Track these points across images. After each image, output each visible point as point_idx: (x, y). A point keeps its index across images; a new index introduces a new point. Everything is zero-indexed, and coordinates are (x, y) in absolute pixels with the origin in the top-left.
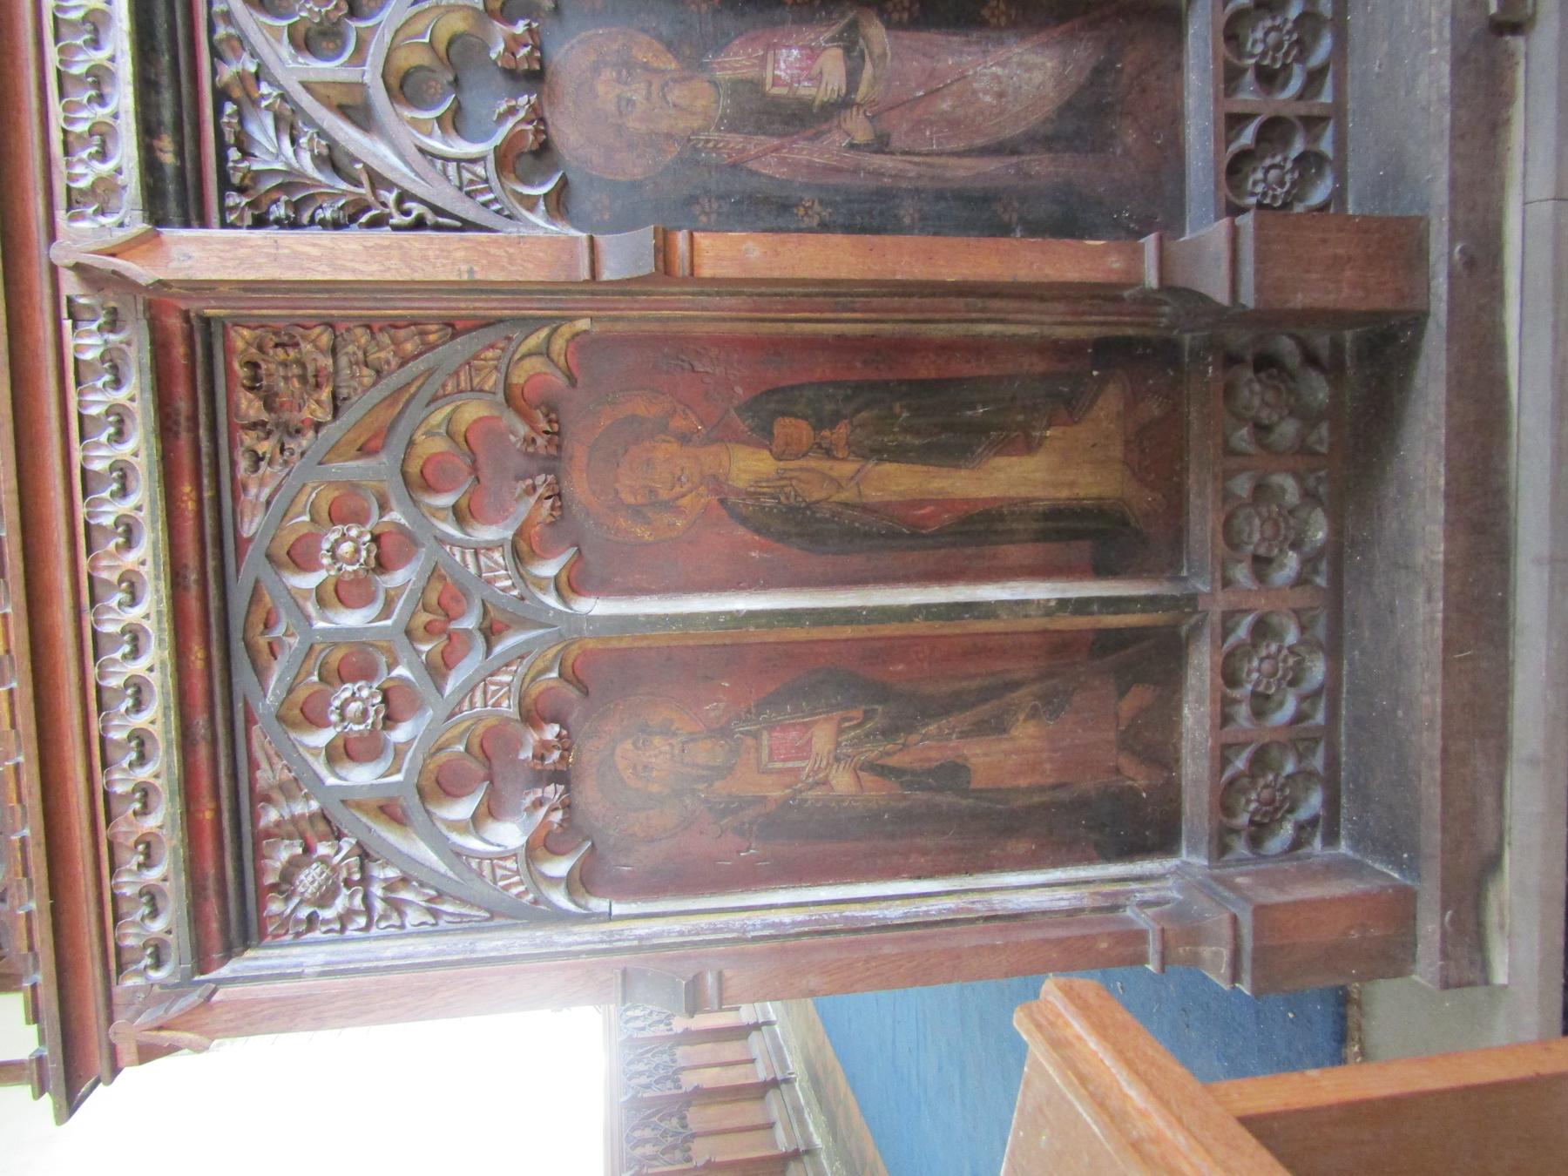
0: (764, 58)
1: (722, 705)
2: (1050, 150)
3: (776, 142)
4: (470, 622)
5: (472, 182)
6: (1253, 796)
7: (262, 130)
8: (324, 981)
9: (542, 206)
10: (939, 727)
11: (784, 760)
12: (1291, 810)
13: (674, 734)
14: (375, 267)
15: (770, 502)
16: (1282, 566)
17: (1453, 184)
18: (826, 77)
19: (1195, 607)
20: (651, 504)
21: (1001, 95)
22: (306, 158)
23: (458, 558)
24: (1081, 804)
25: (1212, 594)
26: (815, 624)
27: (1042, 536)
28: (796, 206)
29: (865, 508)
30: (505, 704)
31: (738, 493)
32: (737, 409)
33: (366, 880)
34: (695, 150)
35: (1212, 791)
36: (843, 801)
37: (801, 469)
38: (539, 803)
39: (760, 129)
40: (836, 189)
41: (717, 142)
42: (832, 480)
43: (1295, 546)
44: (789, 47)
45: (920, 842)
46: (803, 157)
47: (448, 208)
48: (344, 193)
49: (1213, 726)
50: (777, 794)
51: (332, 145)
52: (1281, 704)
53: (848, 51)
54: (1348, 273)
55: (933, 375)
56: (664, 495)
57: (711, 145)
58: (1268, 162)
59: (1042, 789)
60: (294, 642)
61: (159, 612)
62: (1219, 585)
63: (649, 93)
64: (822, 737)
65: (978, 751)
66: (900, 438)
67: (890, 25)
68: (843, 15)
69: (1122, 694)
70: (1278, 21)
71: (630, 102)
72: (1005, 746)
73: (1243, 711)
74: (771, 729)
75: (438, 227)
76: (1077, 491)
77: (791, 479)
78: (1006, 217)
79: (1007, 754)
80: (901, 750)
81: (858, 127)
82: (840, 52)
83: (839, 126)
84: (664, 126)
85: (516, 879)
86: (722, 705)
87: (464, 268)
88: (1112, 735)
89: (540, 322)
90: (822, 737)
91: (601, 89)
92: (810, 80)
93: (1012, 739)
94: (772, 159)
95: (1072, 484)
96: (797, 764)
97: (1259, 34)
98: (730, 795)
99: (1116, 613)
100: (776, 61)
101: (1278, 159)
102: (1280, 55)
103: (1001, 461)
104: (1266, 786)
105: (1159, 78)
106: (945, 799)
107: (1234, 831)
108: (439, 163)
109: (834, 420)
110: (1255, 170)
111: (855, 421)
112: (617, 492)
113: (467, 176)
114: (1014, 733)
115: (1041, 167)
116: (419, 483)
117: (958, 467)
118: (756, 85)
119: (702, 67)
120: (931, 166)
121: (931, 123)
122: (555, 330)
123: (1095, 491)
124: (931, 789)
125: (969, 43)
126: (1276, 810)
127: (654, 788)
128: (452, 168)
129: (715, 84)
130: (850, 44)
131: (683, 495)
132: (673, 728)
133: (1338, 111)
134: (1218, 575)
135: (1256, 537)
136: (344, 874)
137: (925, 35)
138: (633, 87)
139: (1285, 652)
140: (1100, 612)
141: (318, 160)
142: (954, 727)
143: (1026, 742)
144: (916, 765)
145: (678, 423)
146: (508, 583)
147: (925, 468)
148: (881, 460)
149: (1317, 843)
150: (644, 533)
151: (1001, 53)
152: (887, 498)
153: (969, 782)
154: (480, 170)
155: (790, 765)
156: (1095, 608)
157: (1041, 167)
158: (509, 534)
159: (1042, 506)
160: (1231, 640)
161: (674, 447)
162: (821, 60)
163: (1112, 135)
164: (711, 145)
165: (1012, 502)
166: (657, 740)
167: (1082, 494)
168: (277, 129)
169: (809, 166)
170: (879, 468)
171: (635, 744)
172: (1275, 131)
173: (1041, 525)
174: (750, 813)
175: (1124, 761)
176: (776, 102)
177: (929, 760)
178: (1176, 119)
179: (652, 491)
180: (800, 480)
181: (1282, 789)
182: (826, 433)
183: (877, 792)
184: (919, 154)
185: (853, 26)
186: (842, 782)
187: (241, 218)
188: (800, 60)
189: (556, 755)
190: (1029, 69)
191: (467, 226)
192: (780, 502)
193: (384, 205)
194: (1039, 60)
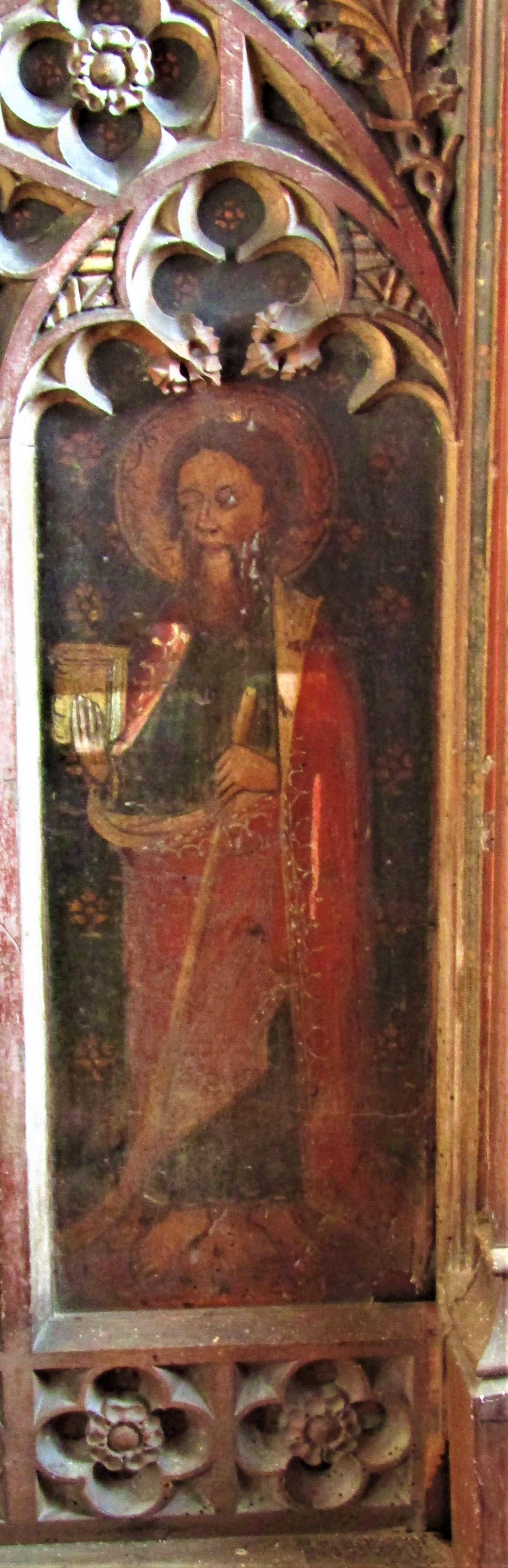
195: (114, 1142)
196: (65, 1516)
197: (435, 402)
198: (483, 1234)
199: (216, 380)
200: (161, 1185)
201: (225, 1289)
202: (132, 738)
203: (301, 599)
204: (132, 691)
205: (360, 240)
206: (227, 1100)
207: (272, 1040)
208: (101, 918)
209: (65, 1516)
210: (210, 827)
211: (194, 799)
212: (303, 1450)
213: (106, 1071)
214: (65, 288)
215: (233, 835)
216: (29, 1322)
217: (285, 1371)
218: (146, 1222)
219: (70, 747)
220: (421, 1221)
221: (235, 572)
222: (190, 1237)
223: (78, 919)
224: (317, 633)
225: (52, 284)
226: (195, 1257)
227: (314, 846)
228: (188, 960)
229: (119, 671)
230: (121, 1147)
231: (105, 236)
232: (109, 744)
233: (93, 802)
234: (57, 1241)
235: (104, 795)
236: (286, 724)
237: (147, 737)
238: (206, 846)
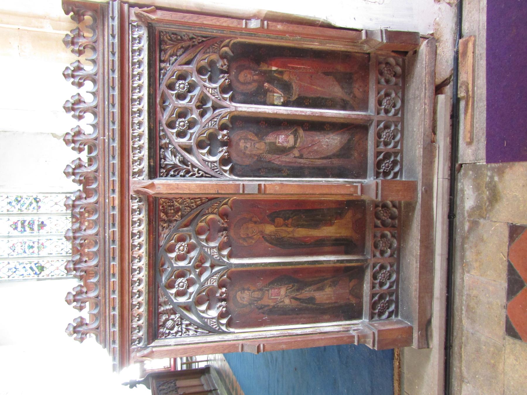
0: (276, 137)
2: (338, 158)
3: (278, 156)
4: (207, 264)
5: (214, 167)
6: (379, 305)
7: (168, 154)
8: (176, 347)
9: (228, 172)
12: (388, 309)
13: (250, 290)
15: (273, 237)
16: (387, 252)
17: (423, 175)
20: (248, 237)
21: (328, 146)
22: (177, 161)
23: (206, 250)
24: (340, 307)
25: (371, 259)
26: (283, 265)
27: (333, 245)
28: (282, 170)
29: (294, 238)
30: (215, 283)
31: (267, 235)
32: (267, 216)
33: (181, 324)
34: (261, 158)
35: (370, 303)
37: (281, 229)
38: (220, 306)
39: (275, 153)
40: (291, 167)
43: (390, 248)
44: (282, 135)
45: (304, 315)
46: (284, 160)
47: (208, 173)
48: (185, 168)
49: (370, 289)
50: (272, 304)
51: (184, 158)
52: (386, 284)
53: (295, 136)
54: (401, 193)
55: (311, 208)
56: (250, 235)
58: (386, 162)
59: (332, 303)
60: (170, 269)
61: (146, 264)
62: (372, 257)
63: (251, 145)
64: (283, 291)
66: (303, 222)
67: (304, 130)
68: (294, 128)
69: (350, 281)
70: (389, 131)
72: (324, 293)
73: (377, 285)
74: (271, 289)
75: (206, 177)
78: (328, 173)
79: (324, 295)
81: (296, 153)
82: (293, 136)
83: (292, 152)
84: (254, 152)
85: (215, 324)
87: (216, 190)
88: (348, 291)
89: (227, 198)
90: (283, 291)
91: (241, 144)
92: (286, 142)
94: (277, 160)
95: (340, 233)
96: (277, 297)
97: (385, 133)
98: (262, 305)
100: (279, 138)
101: (388, 161)
102: (389, 138)
103: (325, 228)
104: (382, 303)
105: (362, 142)
106: (310, 306)
107: (375, 314)
108: (207, 163)
109: (289, 218)
110: (383, 164)
111: (293, 218)
112: (240, 234)
113: (213, 165)
114: (326, 290)
115: (336, 162)
116: (199, 233)
117: (315, 229)
118: (274, 143)
119: (263, 140)
120: (312, 161)
121: (312, 152)
122: (229, 199)
123: (345, 235)
124: (306, 303)
125: (321, 134)
126: (384, 309)
127: (245, 303)
128: (209, 164)
129: (265, 143)
130: (295, 134)
131: (254, 235)
133: (401, 151)
134: (372, 254)
135: (381, 245)
136: (177, 323)
137: (311, 132)
139: (387, 272)
140: (346, 263)
141: (180, 162)
143: (328, 292)
144: (304, 298)
145: (254, 219)
146: (217, 256)
148: (298, 228)
149: (393, 316)
150: (245, 244)
151: (328, 136)
152: (299, 236)
154: (215, 164)
156: (345, 262)
158: (217, 245)
159: (333, 238)
160: (375, 269)
161: (253, 225)
163: (352, 155)
165: (327, 237)
166: (246, 291)
167: (342, 235)
168: (171, 154)
169: (285, 161)
170: (298, 229)
171: (241, 292)
172: (387, 156)
173: (334, 242)
174: (266, 309)
175: (350, 297)
176: (278, 147)
177: (307, 296)
178: (366, 151)
179: (248, 235)
180: (280, 232)
181: (386, 304)
182: (286, 221)
183: (295, 303)
184: (309, 159)
185: (296, 130)
186: (287, 301)
187: (163, 174)
189: (225, 295)
190: (334, 139)
191: (212, 176)
193: (194, 171)
194: (336, 138)
196: (400, 113)
197: (232, 42)
198: (360, 41)
199: (228, 75)
200: (349, 94)
201: (366, 86)
202: (281, 93)
203: (261, 65)
204: (274, 92)
205: (208, 51)
206: (337, 83)
207: (328, 75)
209: (400, 113)
210: (295, 82)
211: (291, 84)
212: (392, 75)
213: (332, 101)
214: (214, 96)
216: (370, 115)
217: (379, 76)
218: (355, 97)
219: (282, 102)
220: (357, 54)
221: (257, 75)
222: (357, 90)
223: (308, 103)
224: (266, 63)
225: (213, 98)
226: (361, 90)
227: (299, 66)
228: (315, 87)
229: (271, 94)
231: (206, 89)
232: (282, 96)
233: (291, 100)
234: (357, 111)
235: (289, 98)
236: (280, 69)
237: (281, 90)
238: (298, 83)
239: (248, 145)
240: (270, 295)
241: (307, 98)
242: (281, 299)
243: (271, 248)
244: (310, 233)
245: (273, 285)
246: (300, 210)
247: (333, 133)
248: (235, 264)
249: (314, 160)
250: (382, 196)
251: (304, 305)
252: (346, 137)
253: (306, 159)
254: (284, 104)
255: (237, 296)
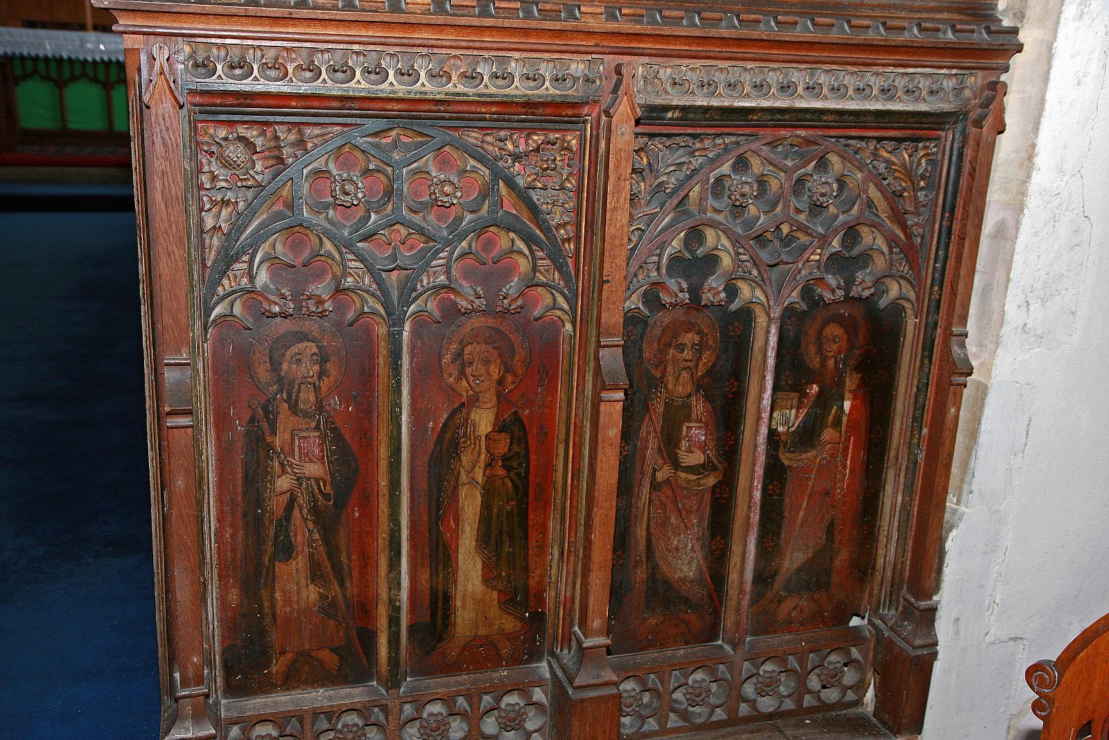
1: (338, 407)
3: (658, 429)
10: (317, 540)
11: (300, 446)
13: (320, 378)
14: (612, 231)
15: (461, 432)
18: (690, 455)
19: (391, 688)
20: (464, 364)
21: (677, 549)
24: (263, 633)
27: (434, 593)
29: (456, 488)
31: (468, 414)
32: (515, 413)
36: (271, 484)
37: (480, 448)
41: (660, 398)
42: (474, 467)
44: (706, 435)
46: (651, 445)
53: (703, 466)
56: (468, 370)
57: (659, 394)
61: (426, 93)
63: (687, 361)
64: (313, 469)
65: (300, 565)
67: (714, 487)
68: (720, 462)
69: (333, 650)
71: (682, 351)
72: (303, 582)
76: (460, 610)
77: (475, 444)
79: (298, 583)
80: (303, 517)
86: (338, 407)
87: (610, 278)
90: (313, 469)
91: (690, 335)
93: (307, 586)
95: (464, 607)
98: (278, 413)
99: (389, 642)
103: (479, 565)
106: (269, 548)
109: (508, 468)
114: (311, 587)
119: (697, 391)
121: (665, 513)
123: (459, 621)
124: (276, 536)
127: (285, 366)
129: (690, 395)
132: (324, 377)
138: (690, 352)
142: (316, 549)
143: (304, 594)
145: (509, 378)
147: (477, 521)
148: (483, 495)
150: (447, 358)
151: (697, 548)
153: (279, 561)
155: (297, 450)
157: (641, 574)
161: (496, 376)
162: (698, 451)
164: (659, 394)
165: (455, 572)
166: (317, 368)
170: (478, 494)
171: (315, 354)
173: (441, 594)
175: (289, 656)
177: (295, 535)
179: (471, 364)
183: (276, 505)
185: (715, 468)
186: (284, 483)
188: (699, 441)
192: (461, 438)
195: (773, 573)
197: (907, 305)
200: (786, 588)
202: (796, 426)
203: (855, 375)
204: (798, 408)
206: (811, 555)
208: (778, 491)
210: (817, 456)
211: (813, 447)
213: (773, 547)
215: (824, 459)
221: (835, 366)
222: (793, 607)
224: (858, 387)
227: (848, 462)
228: (804, 505)
229: (795, 402)
230: (774, 575)
233: (781, 449)
235: (785, 446)
236: (845, 419)
238: (815, 463)
239: (687, 354)
240: (305, 434)
241: (783, 487)
242: (291, 466)
243: (433, 429)
244: (467, 528)
245: (331, 442)
246: (526, 494)
247: (705, 558)
248: (400, 333)
249: (645, 520)
250: (583, 701)
251: (272, 532)
252: (697, 593)
253: (650, 498)
254: (772, 433)
255: (305, 344)
